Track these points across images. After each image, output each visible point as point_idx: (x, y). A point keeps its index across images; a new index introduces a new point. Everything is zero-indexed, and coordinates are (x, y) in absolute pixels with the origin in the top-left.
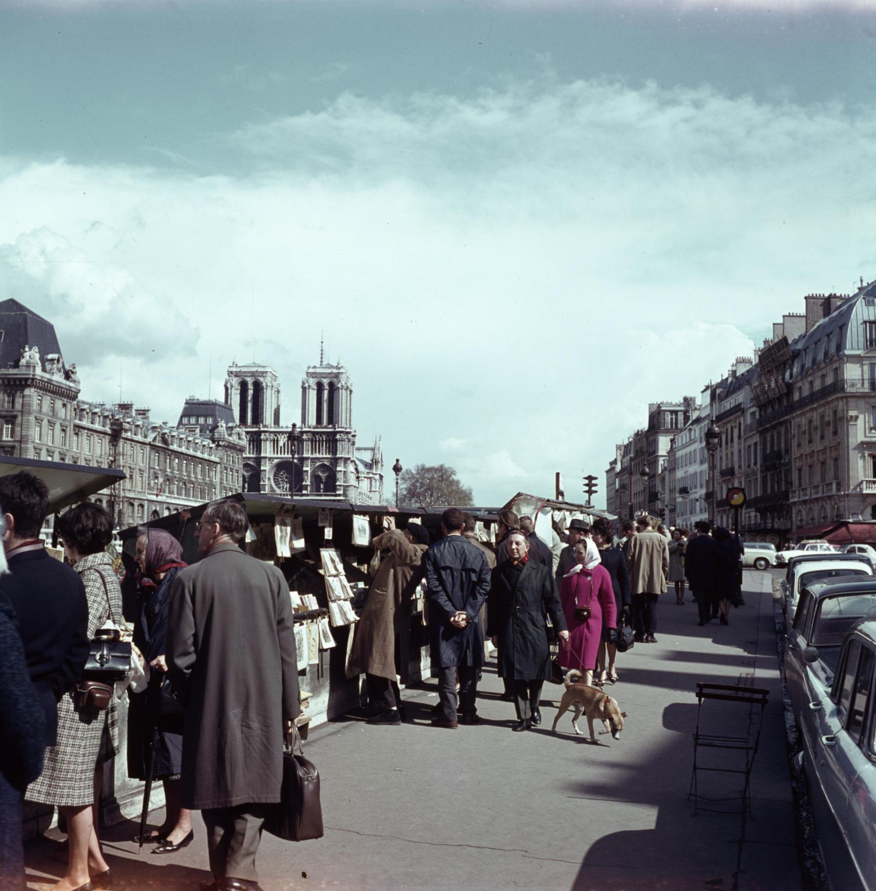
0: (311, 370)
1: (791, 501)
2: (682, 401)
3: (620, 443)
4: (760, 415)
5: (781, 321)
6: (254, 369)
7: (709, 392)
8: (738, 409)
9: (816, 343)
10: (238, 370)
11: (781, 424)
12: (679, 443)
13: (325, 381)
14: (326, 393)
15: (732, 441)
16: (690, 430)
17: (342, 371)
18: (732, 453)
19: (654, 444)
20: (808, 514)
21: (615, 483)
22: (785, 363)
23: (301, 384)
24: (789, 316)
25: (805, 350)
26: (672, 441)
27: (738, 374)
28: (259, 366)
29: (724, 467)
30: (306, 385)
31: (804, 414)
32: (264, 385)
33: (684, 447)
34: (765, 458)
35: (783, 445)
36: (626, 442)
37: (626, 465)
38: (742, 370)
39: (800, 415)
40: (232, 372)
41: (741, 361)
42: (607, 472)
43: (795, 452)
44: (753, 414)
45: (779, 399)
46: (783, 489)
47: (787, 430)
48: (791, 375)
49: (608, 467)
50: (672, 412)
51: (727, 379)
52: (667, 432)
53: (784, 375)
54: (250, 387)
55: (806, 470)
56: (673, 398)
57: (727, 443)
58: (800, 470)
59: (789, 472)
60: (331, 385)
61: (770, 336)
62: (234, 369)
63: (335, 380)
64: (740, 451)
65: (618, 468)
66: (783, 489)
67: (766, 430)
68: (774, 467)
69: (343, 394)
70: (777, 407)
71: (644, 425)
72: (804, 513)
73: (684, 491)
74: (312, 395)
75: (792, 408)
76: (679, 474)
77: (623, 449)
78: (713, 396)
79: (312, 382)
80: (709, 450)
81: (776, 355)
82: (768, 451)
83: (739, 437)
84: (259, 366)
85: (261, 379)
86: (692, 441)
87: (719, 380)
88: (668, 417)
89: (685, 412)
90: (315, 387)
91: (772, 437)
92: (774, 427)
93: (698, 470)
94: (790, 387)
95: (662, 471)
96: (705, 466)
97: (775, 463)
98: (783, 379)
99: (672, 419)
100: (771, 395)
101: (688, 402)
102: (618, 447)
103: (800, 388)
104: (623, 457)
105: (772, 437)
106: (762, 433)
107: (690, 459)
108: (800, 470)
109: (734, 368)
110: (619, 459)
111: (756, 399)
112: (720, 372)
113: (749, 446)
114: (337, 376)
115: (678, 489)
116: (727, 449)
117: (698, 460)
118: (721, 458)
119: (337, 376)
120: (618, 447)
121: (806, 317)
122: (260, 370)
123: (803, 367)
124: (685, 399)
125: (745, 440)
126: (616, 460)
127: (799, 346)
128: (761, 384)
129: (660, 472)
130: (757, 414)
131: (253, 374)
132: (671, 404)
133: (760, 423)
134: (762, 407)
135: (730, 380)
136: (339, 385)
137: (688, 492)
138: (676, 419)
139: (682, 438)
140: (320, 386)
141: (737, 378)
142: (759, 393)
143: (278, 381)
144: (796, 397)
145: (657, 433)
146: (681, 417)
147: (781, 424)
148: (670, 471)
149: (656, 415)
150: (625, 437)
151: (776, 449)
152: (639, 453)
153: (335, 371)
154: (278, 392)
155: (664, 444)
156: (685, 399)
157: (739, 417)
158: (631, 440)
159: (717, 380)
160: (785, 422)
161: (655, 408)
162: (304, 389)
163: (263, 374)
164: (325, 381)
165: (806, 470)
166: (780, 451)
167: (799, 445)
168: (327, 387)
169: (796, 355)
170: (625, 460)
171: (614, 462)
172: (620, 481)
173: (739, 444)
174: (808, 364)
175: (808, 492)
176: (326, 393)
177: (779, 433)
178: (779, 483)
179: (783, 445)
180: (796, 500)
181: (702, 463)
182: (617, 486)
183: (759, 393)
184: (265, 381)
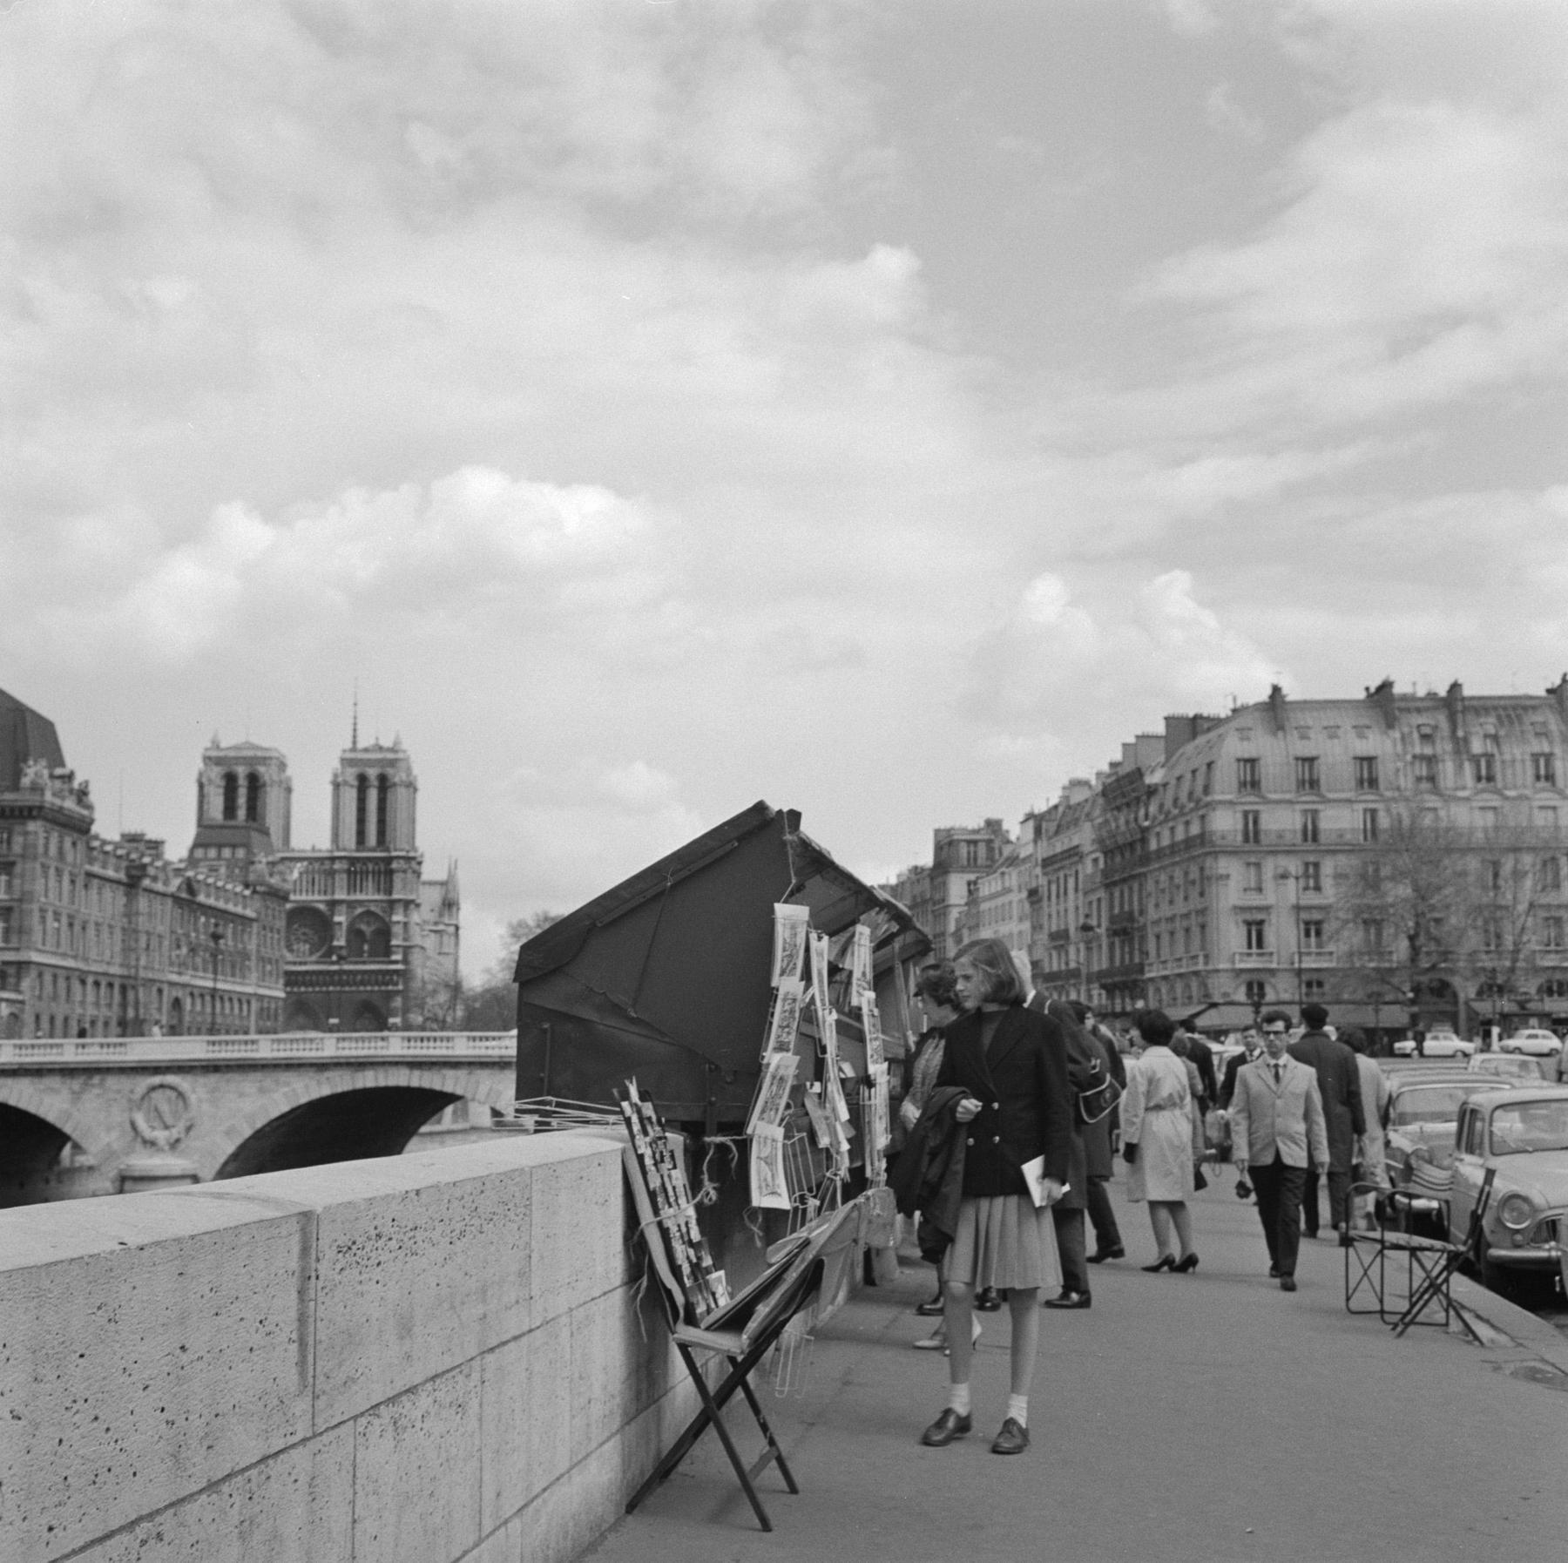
1: (1148, 975)
7: (1031, 824)
8: (1074, 853)
11: (1133, 877)
13: (372, 773)
17: (401, 755)
22: (1138, 799)
29: (1054, 928)
34: (1112, 919)
35: (1136, 903)
38: (1078, 796)
41: (1076, 784)
43: (1152, 914)
44: (1096, 861)
45: (1131, 845)
46: (1137, 960)
48: (1146, 817)
50: (969, 842)
52: (963, 870)
55: (1165, 938)
56: (969, 819)
57: (1058, 896)
58: (1158, 937)
59: (1143, 939)
60: (383, 778)
63: (390, 771)
66: (1137, 960)
67: (1115, 884)
70: (1127, 855)
71: (927, 859)
72: (1164, 991)
74: (350, 796)
75: (1146, 859)
78: (1038, 831)
81: (1124, 788)
82: (1116, 911)
83: (1076, 890)
88: (963, 850)
90: (356, 783)
92: (1124, 880)
93: (1015, 931)
95: (958, 930)
96: (1026, 926)
98: (1136, 819)
100: (1121, 840)
101: (993, 825)
103: (1158, 834)
106: (1109, 886)
107: (1003, 915)
108: (1158, 937)
111: (1100, 841)
113: (1090, 903)
114: (393, 763)
118: (1050, 916)
123: (1161, 806)
124: (989, 823)
125: (1086, 894)
132: (964, 830)
134: (1108, 853)
135: (1061, 809)
136: (397, 780)
140: (362, 780)
141: (1069, 807)
144: (1153, 845)
146: (982, 850)
147: (1133, 877)
148: (970, 929)
149: (946, 844)
151: (1126, 908)
153: (390, 756)
157: (1076, 863)
159: (1041, 807)
163: (264, 760)
164: (372, 773)
165: (1165, 938)
166: (1131, 913)
167: (1157, 905)
168: (376, 783)
169: (1152, 791)
173: (1077, 899)
174: (1168, 804)
175: (1169, 965)
177: (1131, 889)
178: (1131, 953)
179: (1136, 903)
180: (1152, 975)
181: (1021, 920)
183: (1105, 834)
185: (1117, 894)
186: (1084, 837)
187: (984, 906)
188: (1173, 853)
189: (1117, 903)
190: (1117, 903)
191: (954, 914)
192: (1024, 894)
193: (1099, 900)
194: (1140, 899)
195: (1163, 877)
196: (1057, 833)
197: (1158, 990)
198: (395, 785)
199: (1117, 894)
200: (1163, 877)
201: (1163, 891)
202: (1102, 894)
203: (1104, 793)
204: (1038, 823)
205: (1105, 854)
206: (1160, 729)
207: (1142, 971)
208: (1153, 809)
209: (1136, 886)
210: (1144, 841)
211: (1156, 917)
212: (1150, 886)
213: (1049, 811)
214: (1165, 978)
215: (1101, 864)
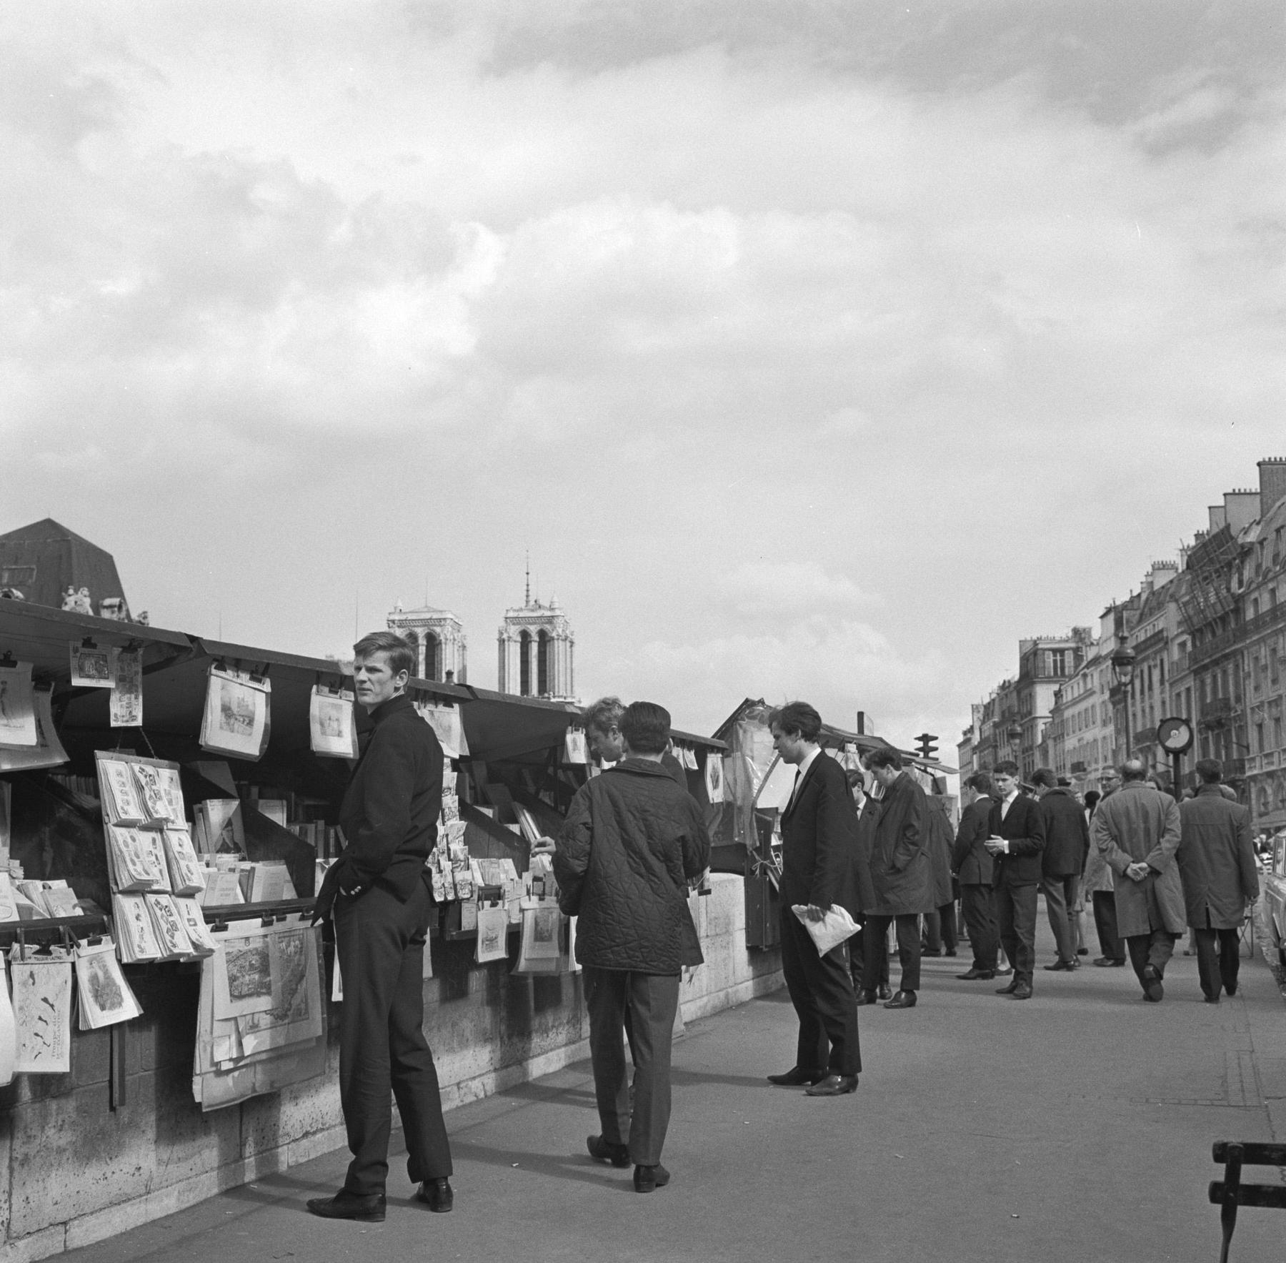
0: (511, 614)
1: (1248, 774)
2: (1070, 634)
3: (977, 701)
4: (1194, 645)
5: (1222, 503)
6: (428, 616)
7: (1111, 617)
8: (1159, 639)
9: (1278, 531)
10: (403, 617)
11: (1226, 657)
12: (1068, 697)
13: (533, 630)
14: (534, 648)
15: (1150, 688)
16: (1085, 676)
17: (557, 613)
18: (1152, 708)
19: (1031, 697)
20: (1275, 793)
21: (971, 762)
22: (1229, 565)
23: (497, 636)
24: (1234, 493)
25: (1261, 543)
26: (1058, 695)
27: (1156, 588)
28: (435, 611)
29: (1139, 729)
30: (505, 636)
31: (1263, 640)
32: (442, 638)
33: (1075, 702)
34: (1204, 711)
35: (1231, 689)
36: (987, 700)
37: (986, 734)
38: (1161, 580)
39: (1258, 642)
40: (393, 622)
41: (1160, 567)
42: (959, 746)
43: (1251, 699)
44: (1183, 645)
45: (1223, 619)
46: (1235, 756)
47: (1237, 666)
48: (1241, 583)
49: (961, 739)
50: (1055, 651)
51: (1139, 595)
52: (1049, 680)
53: (1229, 582)
54: (422, 641)
55: (1269, 725)
56: (1057, 630)
57: (1142, 692)
58: (1260, 726)
59: (1242, 729)
60: (542, 634)
61: (1204, 526)
62: (396, 617)
63: (547, 627)
64: (1163, 703)
65: (976, 739)
66: (1235, 756)
67: (1205, 668)
68: (1219, 724)
69: (559, 648)
70: (1219, 632)
71: (1013, 673)
72: (1269, 791)
73: (1078, 767)
74: (514, 651)
75: (1243, 632)
76: (1070, 743)
77: (982, 710)
78: (1119, 624)
79: (514, 631)
80: (1114, 704)
81: (1215, 554)
82: (1208, 701)
83: (1162, 682)
84: (435, 611)
85: (438, 630)
86: (1090, 693)
87: (1127, 598)
88: (1050, 659)
89: (1076, 651)
90: (519, 639)
91: (1215, 677)
92: (1216, 663)
93: (1100, 737)
94: (1239, 599)
95: (1044, 741)
96: (1111, 729)
97: (1220, 722)
98: (1228, 589)
99: (1055, 661)
100: (1210, 614)
101: (1080, 635)
102: (975, 708)
103: (1256, 600)
104: (983, 722)
105: (1215, 677)
106: (1198, 672)
107: (1086, 720)
108: (1260, 726)
109: (1150, 579)
110: (977, 725)
111: (1186, 621)
112: (1127, 585)
113: (1178, 695)
114: (550, 620)
115: (1068, 766)
116: (1143, 701)
117: (1099, 722)
118: (1134, 715)
119: (550, 620)
120: (975, 708)
121: (1260, 493)
122: (435, 616)
123: (1259, 566)
124: (1076, 631)
125: (1171, 685)
126: (972, 727)
127: (1252, 537)
128: (1194, 597)
129: (1039, 741)
130: (1189, 644)
131: (425, 623)
132: (1053, 640)
133: (1193, 658)
134: (1196, 633)
135: (1144, 597)
136: (554, 634)
137: (1085, 770)
138: (1062, 661)
139: (1073, 690)
140: (525, 635)
141: (1153, 593)
142: (1191, 612)
143: (463, 632)
144: (1250, 614)
145: (1034, 683)
146: (1069, 658)
147: (1226, 657)
148: (1055, 739)
149: (1031, 658)
150: (985, 690)
151: (1220, 696)
152: (1008, 716)
153: (548, 613)
154: (464, 647)
155: (1044, 699)
156: (1076, 631)
157: (1160, 651)
158: (994, 696)
159: (1122, 598)
160: (1234, 653)
161: (1029, 647)
162: (502, 642)
163: (440, 621)
164: (533, 630)
165: (1269, 725)
166: (1227, 700)
167: (1257, 688)
168: (537, 638)
169: (1246, 552)
170: (985, 727)
171: (971, 730)
172: (980, 758)
173: (1162, 692)
174: (1267, 563)
175: (1275, 759)
176: (534, 648)
177: (1225, 672)
178: (1227, 748)
179: (1231, 689)
180: (1255, 772)
181: (1105, 724)
182: (976, 767)
183: (1191, 612)
184: (444, 633)
185: (1209, 681)
186: (1169, 620)
187: (1068, 714)
188: (1275, 619)
189: (1208, 689)
190: (1208, 689)
191: (1041, 726)
192: (1107, 695)
193: (1188, 690)
194: (1237, 684)
195: (1264, 652)
196: (1140, 621)
197: (1262, 791)
198: (553, 639)
199: (1209, 681)
200: (1264, 652)
201: (1265, 668)
202: (1190, 682)
203: (1189, 566)
204: (1118, 615)
205: (1193, 634)
206: (1252, 482)
207: (1242, 769)
208: (1248, 573)
209: (1231, 667)
210: (1238, 611)
211: (1256, 702)
212: (1248, 665)
213: (1132, 600)
214: (1270, 775)
215: (1189, 647)
